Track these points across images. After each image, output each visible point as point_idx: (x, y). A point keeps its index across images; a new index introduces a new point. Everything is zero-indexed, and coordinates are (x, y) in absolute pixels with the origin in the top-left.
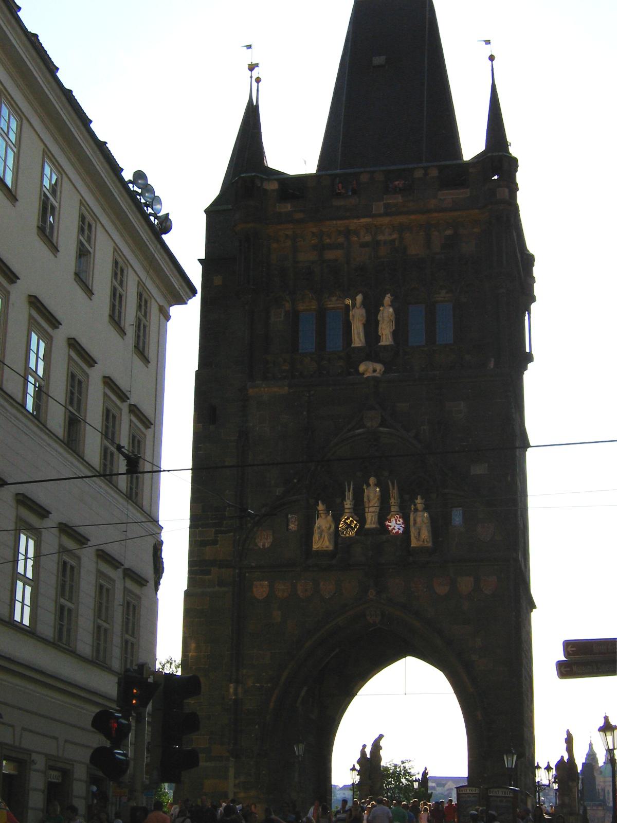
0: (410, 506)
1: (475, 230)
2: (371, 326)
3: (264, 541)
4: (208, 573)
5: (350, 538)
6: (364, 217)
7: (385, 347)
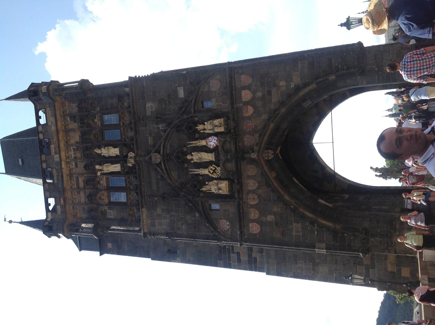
0: (202, 133)
1: (67, 104)
2: (112, 160)
3: (225, 225)
4: (255, 258)
5: (221, 170)
6: (61, 165)
7: (120, 152)
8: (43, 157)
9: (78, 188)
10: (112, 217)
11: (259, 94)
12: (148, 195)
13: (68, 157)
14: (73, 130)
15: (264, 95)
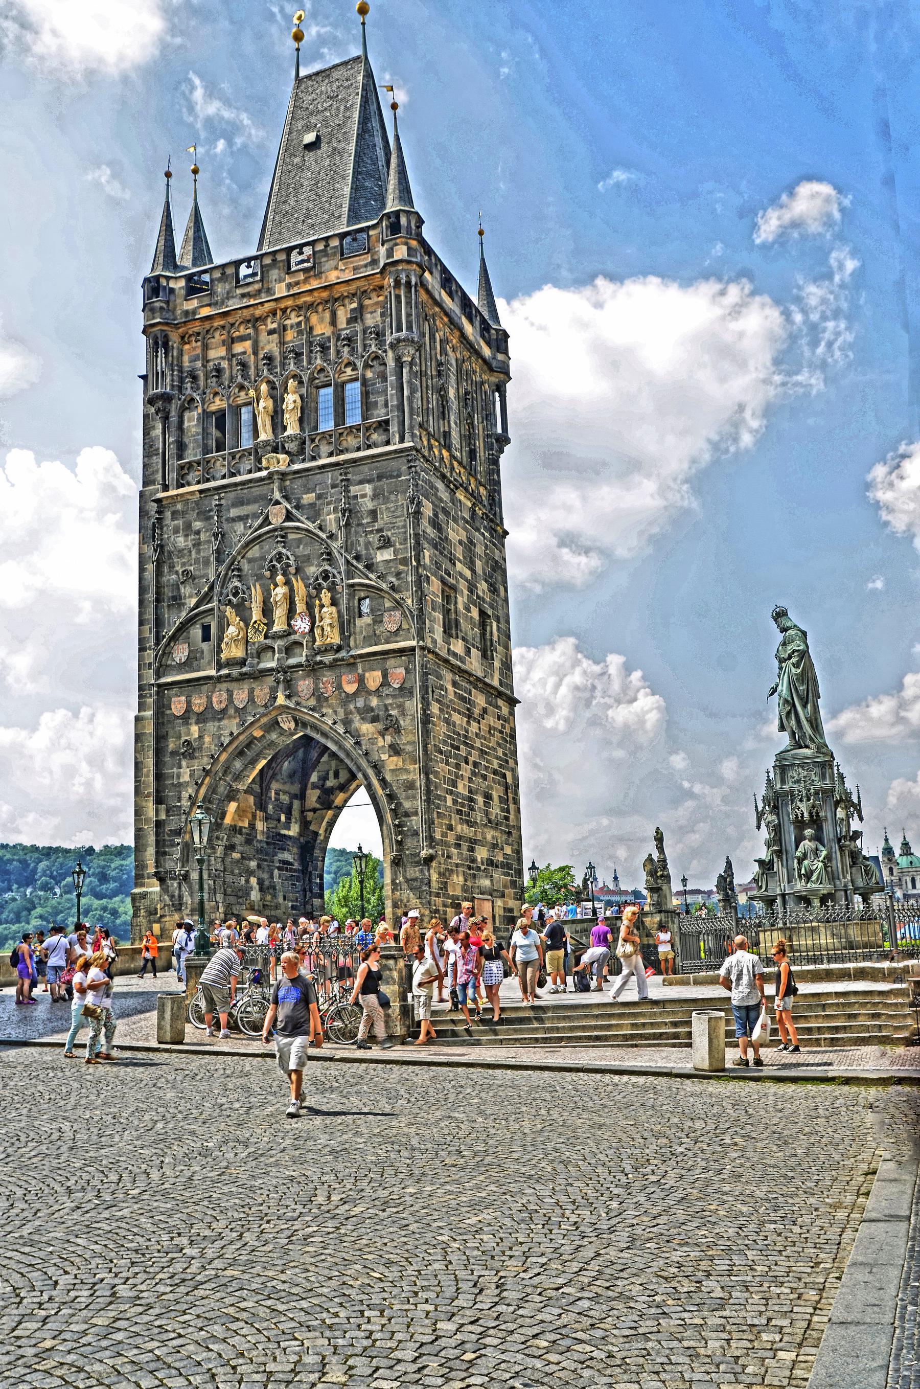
8: (282, 257)
9: (233, 342)
10: (186, 424)
11: (374, 702)
12: (223, 502)
13: (284, 311)
14: (333, 322)
15: (372, 709)
